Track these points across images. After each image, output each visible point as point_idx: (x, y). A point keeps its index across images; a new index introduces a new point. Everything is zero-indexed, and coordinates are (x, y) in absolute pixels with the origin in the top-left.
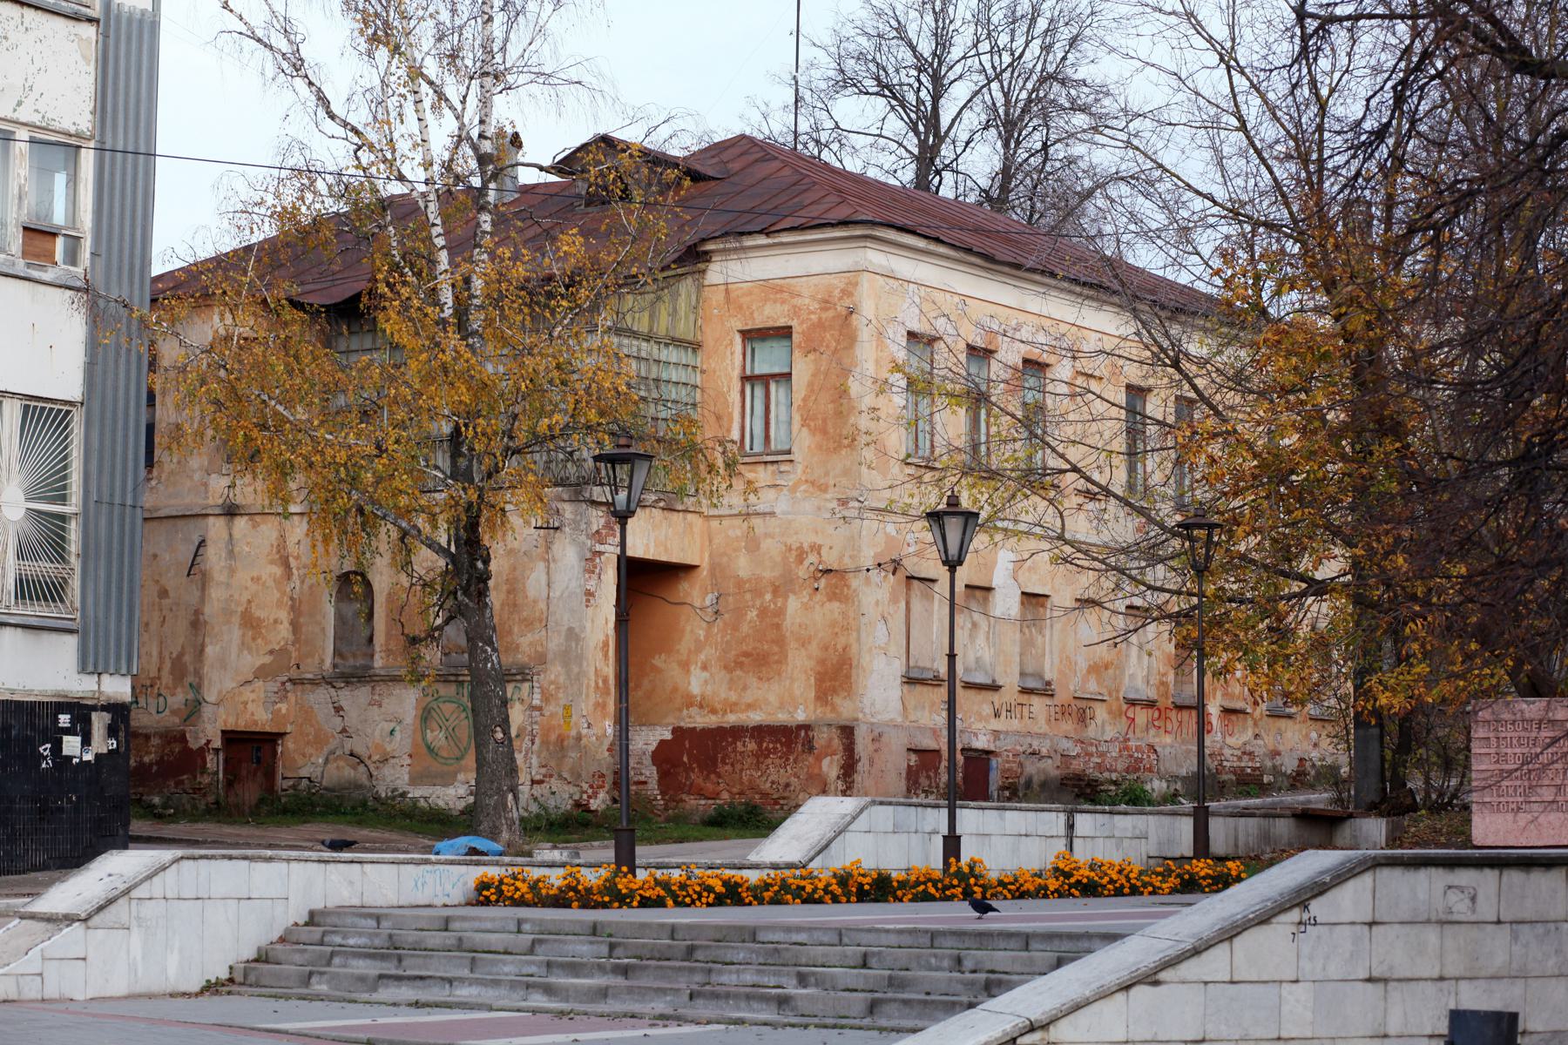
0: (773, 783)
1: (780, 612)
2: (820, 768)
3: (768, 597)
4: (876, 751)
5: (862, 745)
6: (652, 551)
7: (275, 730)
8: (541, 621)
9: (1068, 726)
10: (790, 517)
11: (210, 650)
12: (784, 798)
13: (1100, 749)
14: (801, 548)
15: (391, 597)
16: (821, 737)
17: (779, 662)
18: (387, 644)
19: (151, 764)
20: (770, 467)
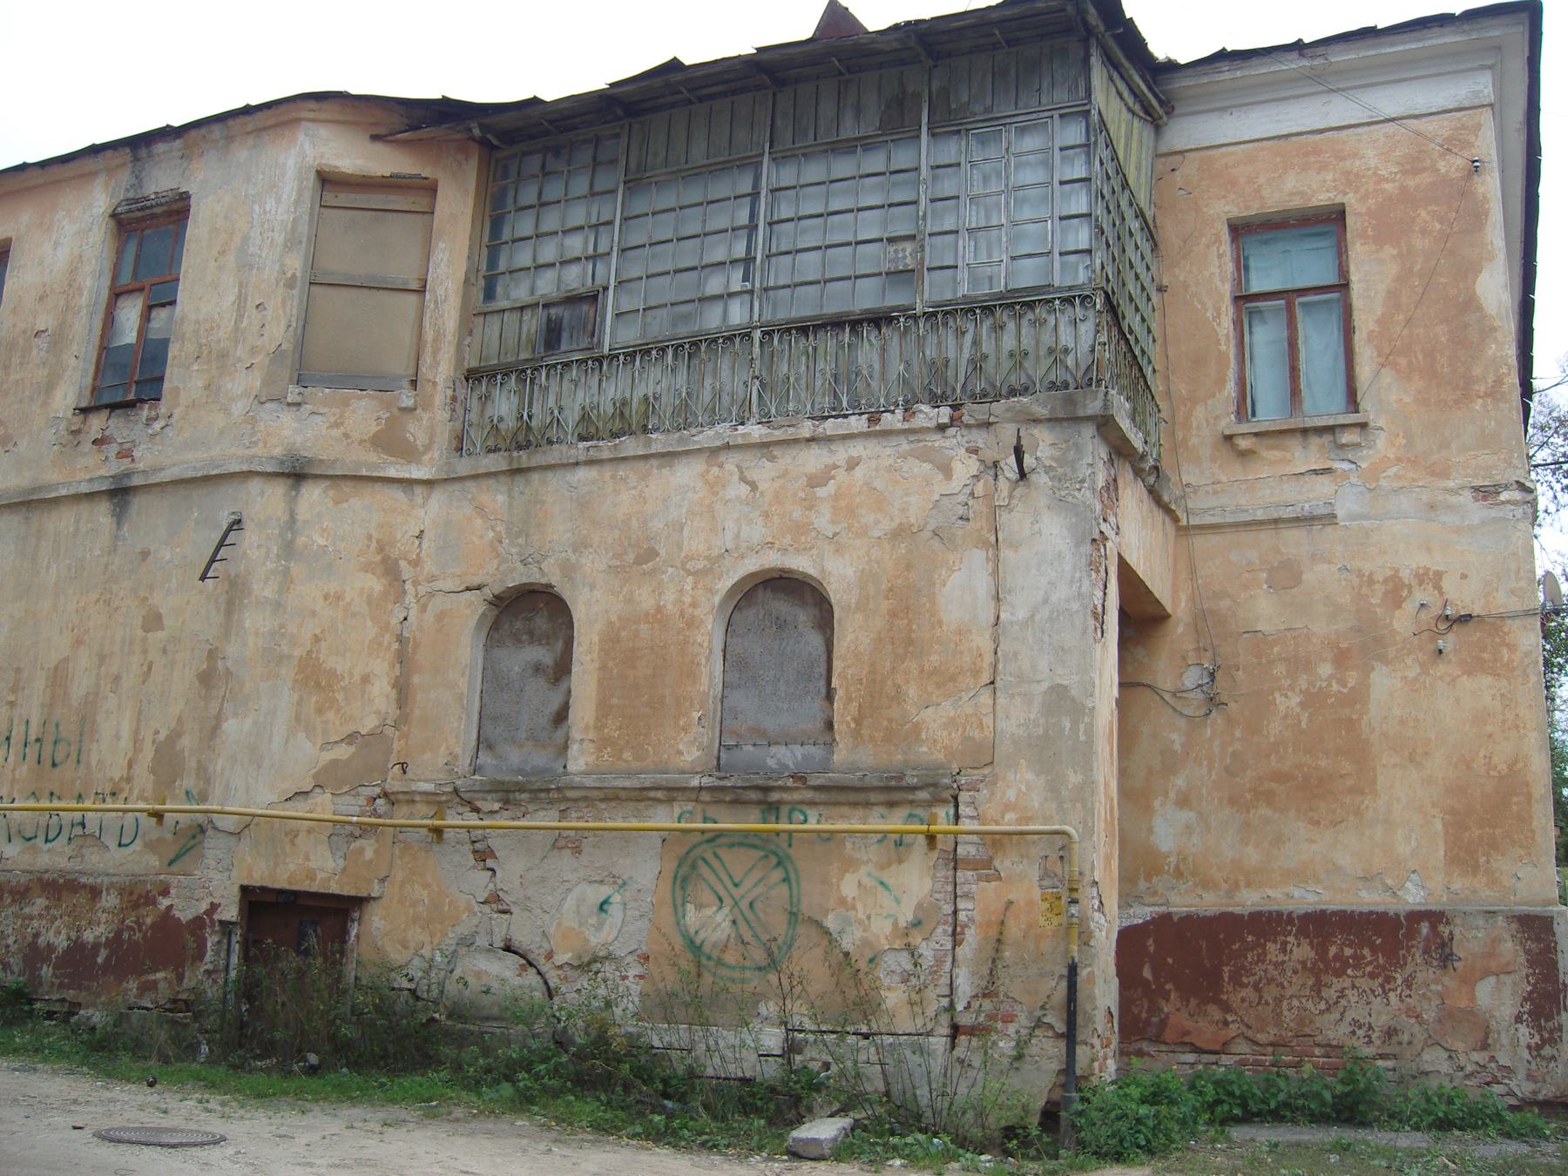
0: (1356, 1023)
1: (1358, 696)
2: (1473, 998)
3: (1325, 669)
7: (348, 891)
8: (976, 673)
10: (1365, 523)
11: (234, 728)
12: (1382, 1057)
15: (611, 639)
16: (1469, 941)
18: (599, 725)
19: (96, 947)
20: (1315, 441)
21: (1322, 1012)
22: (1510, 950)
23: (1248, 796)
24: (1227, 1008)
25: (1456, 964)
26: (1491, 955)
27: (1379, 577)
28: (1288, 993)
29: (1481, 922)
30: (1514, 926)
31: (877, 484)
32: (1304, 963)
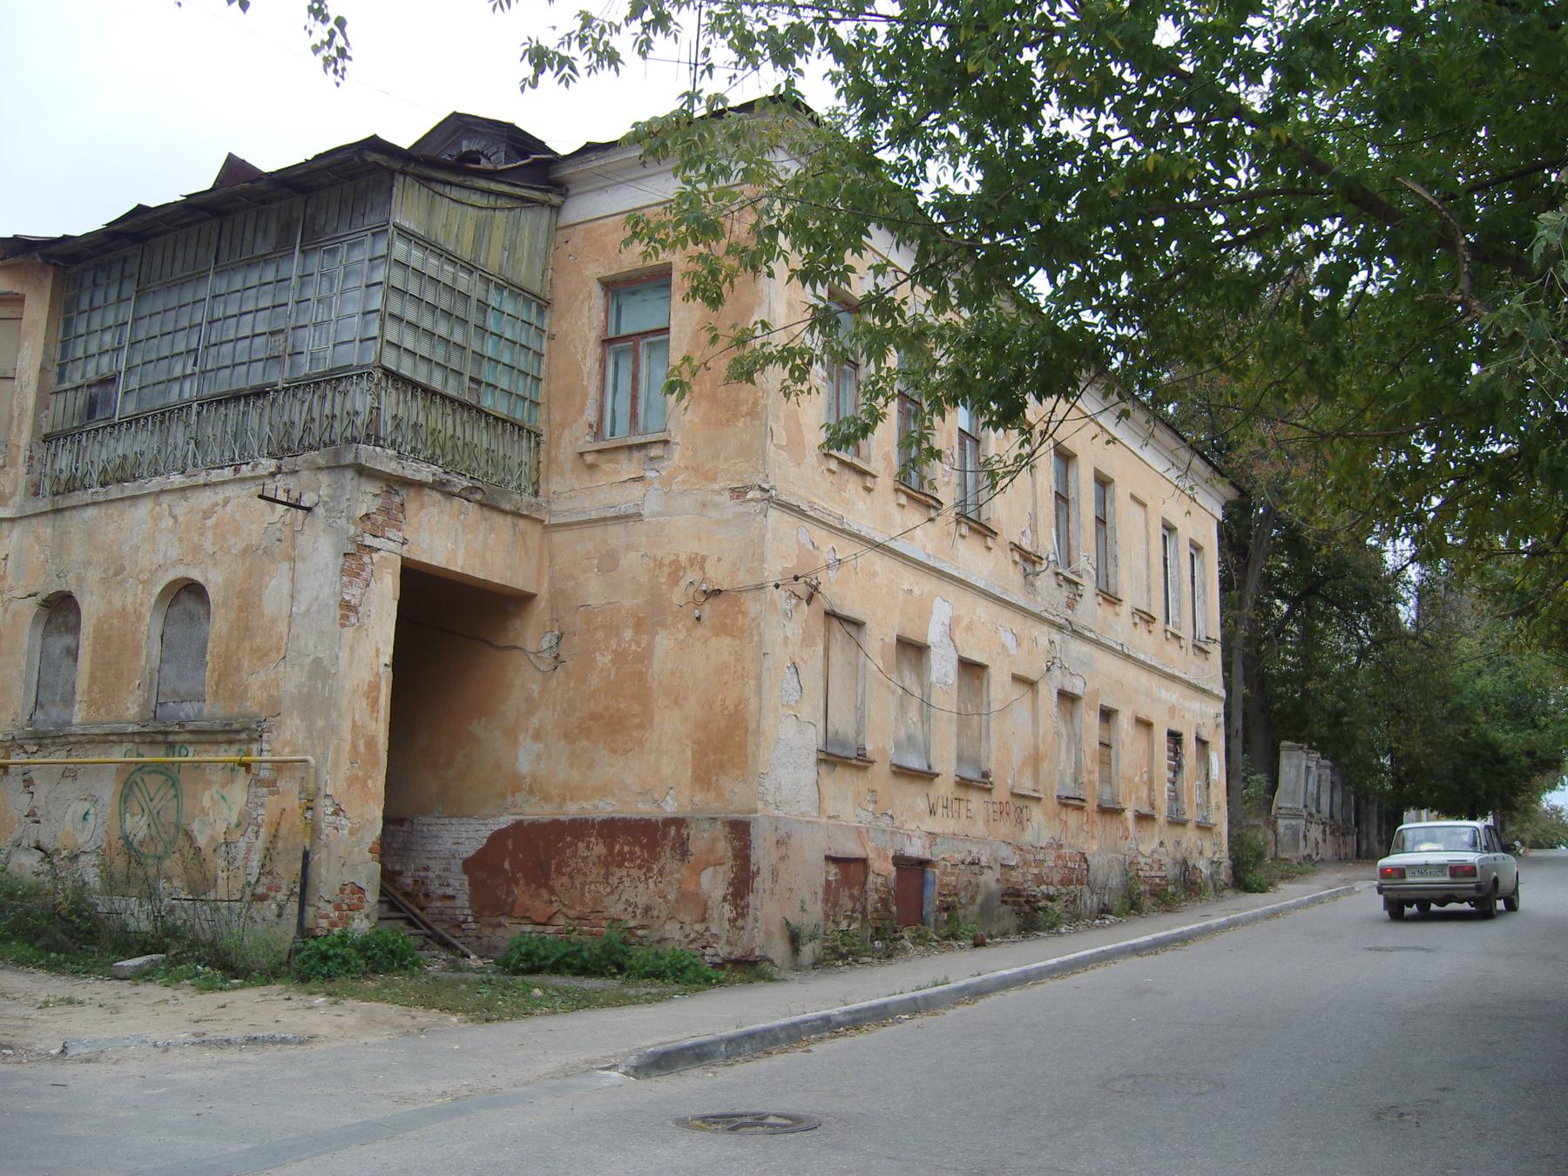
0: (628, 903)
1: (645, 656)
2: (698, 884)
3: (628, 634)
4: (782, 859)
5: (762, 854)
6: (460, 562)
8: (279, 650)
9: (1005, 829)
10: (661, 519)
12: (642, 927)
13: (1038, 857)
15: (99, 629)
16: (699, 839)
17: (642, 727)
18: (90, 691)
20: (636, 455)
22: (724, 847)
23: (576, 731)
25: (691, 858)
26: (711, 851)
27: (666, 561)
29: (707, 827)
30: (727, 829)
31: (237, 517)
32: (599, 857)
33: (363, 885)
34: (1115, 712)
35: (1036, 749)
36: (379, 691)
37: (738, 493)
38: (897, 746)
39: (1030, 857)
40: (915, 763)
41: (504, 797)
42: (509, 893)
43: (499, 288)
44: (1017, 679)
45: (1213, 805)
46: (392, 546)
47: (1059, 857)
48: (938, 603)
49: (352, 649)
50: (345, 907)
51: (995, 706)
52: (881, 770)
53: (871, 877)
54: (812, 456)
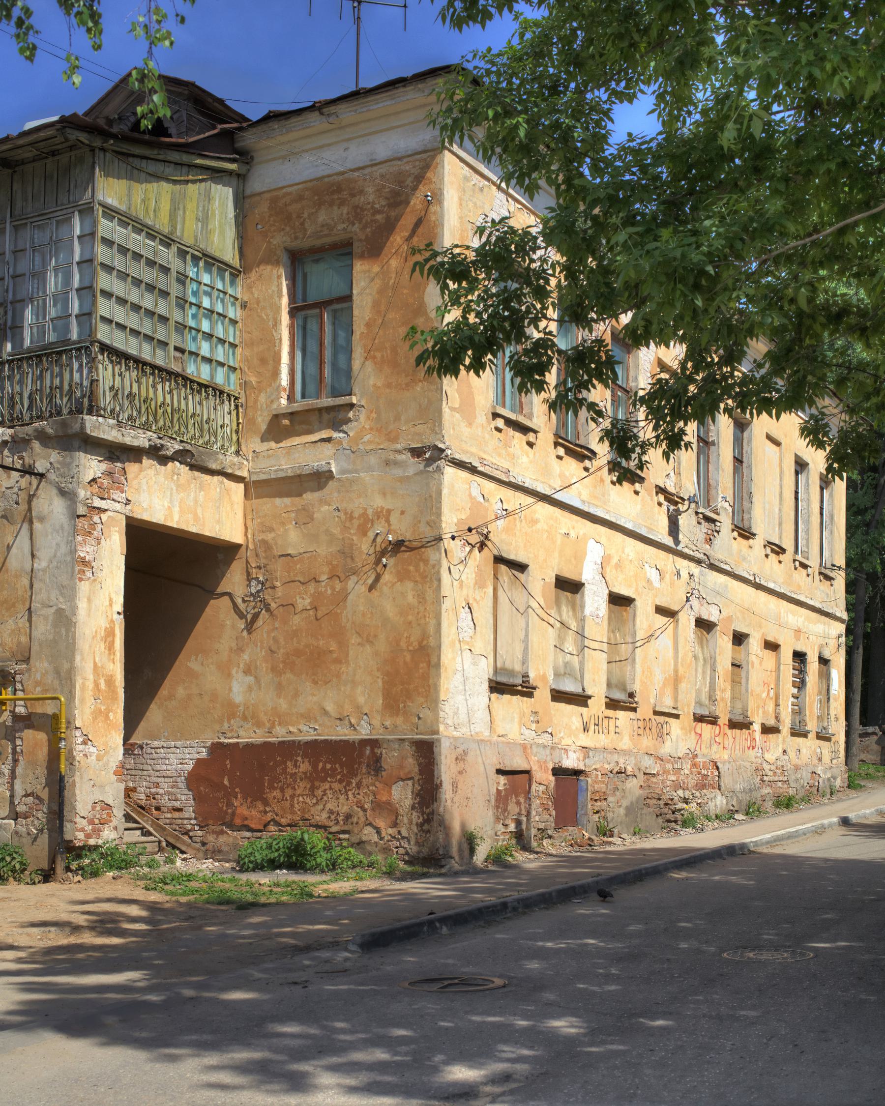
0: (331, 812)
4: (460, 773)
6: (176, 517)
9: (647, 742)
12: (344, 832)
13: (676, 766)
14: (364, 515)
16: (390, 758)
17: (338, 661)
21: (315, 805)
22: (411, 764)
24: (266, 803)
25: (383, 773)
26: (401, 767)
27: (356, 515)
28: (298, 792)
29: (397, 746)
30: (414, 748)
32: (305, 773)
33: (110, 802)
34: (747, 636)
35: (676, 671)
36: (114, 635)
37: (417, 452)
38: (557, 675)
39: (669, 766)
40: (570, 686)
41: (221, 722)
42: (229, 804)
43: (196, 259)
44: (661, 610)
45: (832, 716)
46: (118, 507)
47: (695, 765)
48: (591, 544)
49: (89, 600)
50: (97, 821)
51: (641, 635)
52: (543, 695)
53: (534, 787)
54: (482, 417)
